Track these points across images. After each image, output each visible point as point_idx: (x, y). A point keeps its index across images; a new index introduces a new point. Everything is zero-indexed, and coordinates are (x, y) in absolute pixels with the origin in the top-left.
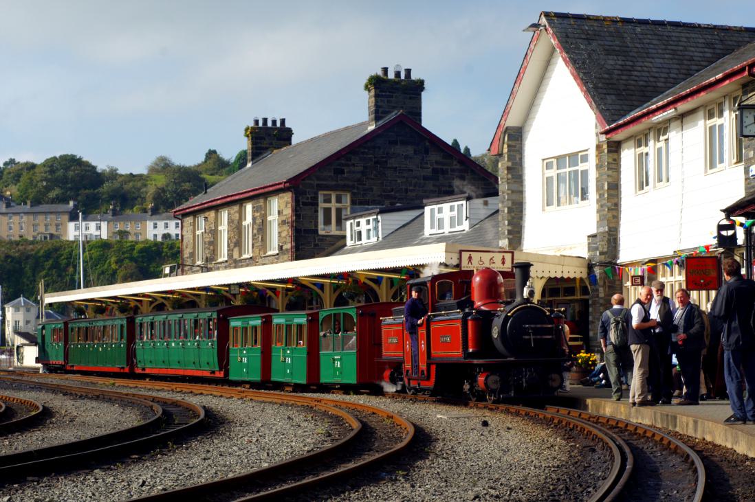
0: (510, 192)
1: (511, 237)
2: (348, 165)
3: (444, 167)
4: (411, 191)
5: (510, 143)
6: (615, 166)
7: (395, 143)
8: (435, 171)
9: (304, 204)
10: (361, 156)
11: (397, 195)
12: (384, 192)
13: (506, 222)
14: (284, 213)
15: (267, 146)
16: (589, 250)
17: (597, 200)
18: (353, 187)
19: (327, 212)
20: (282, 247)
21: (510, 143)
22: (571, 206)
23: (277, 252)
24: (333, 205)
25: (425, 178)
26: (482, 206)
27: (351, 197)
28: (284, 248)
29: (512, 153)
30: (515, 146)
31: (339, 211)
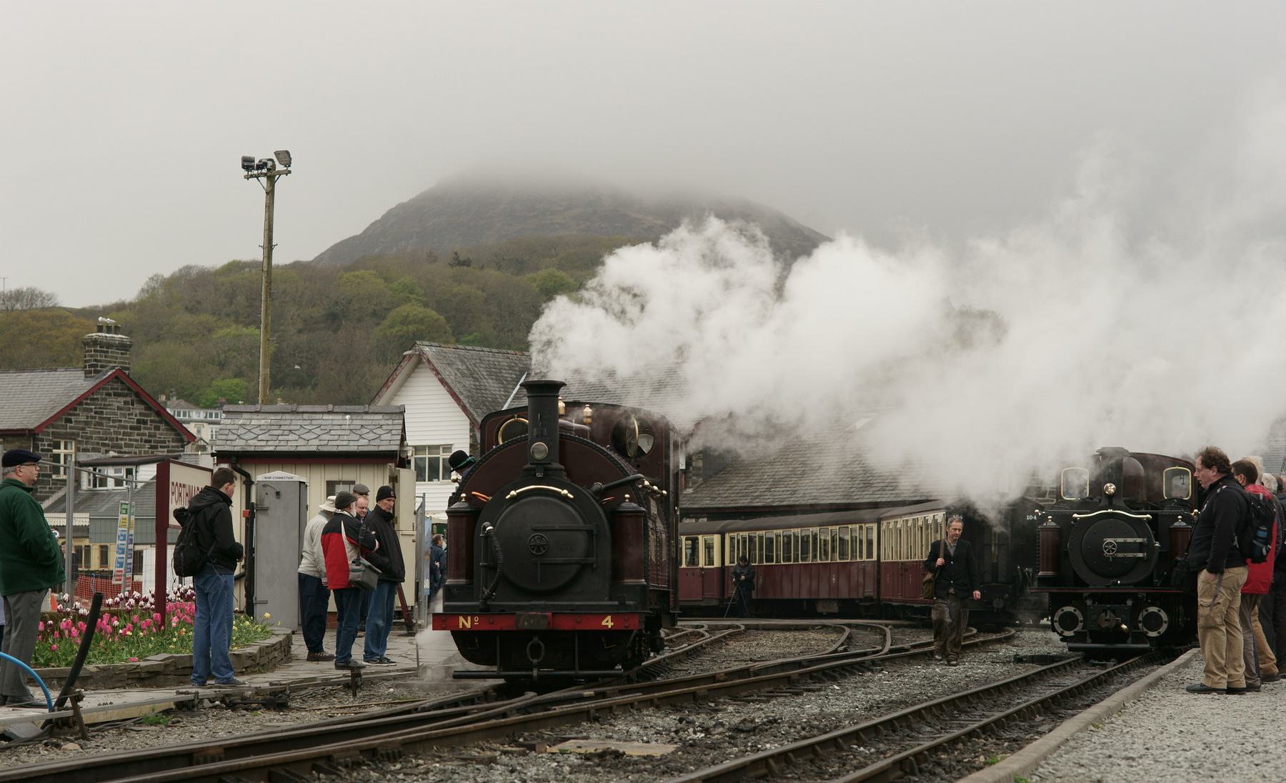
2: (74, 415)
3: (146, 418)
4: (121, 439)
7: (109, 395)
8: (138, 421)
9: (42, 450)
10: (84, 406)
24: (62, 451)
25: (131, 428)
27: (76, 445)
31: (65, 456)
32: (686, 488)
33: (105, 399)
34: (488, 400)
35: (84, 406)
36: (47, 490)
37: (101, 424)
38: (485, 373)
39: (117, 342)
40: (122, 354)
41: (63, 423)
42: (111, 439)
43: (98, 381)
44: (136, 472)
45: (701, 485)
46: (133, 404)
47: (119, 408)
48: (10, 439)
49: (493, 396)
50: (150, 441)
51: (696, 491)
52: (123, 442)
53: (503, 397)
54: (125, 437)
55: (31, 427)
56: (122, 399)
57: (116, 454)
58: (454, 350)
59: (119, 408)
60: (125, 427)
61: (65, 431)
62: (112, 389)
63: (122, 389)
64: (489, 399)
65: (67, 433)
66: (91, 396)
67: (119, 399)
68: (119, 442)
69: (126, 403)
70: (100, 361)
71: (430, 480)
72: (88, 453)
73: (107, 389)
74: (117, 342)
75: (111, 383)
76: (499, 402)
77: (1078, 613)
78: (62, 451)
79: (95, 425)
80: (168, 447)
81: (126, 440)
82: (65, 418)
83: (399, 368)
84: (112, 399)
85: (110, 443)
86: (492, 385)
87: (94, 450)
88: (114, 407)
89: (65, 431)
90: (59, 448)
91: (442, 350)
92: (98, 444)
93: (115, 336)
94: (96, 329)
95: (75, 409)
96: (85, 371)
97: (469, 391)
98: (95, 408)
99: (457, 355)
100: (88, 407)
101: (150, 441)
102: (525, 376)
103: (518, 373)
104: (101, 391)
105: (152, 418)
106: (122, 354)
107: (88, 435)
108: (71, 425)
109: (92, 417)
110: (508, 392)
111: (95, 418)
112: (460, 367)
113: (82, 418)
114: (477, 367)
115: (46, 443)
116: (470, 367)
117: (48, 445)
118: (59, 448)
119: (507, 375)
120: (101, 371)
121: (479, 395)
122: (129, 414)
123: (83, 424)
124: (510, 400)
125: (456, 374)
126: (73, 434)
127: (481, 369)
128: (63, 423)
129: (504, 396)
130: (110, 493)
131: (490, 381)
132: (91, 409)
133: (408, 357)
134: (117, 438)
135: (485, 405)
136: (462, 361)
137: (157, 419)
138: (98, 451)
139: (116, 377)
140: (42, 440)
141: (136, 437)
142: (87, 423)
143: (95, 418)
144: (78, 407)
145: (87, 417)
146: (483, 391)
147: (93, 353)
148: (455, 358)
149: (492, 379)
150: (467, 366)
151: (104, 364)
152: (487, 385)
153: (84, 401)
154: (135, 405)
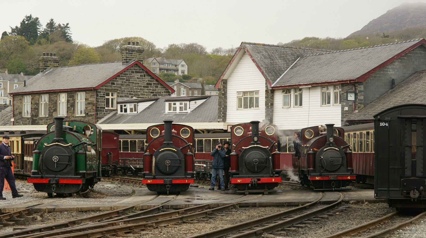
0: (223, 102)
1: (223, 118)
2: (116, 81)
3: (151, 83)
4: (139, 92)
5: (223, 85)
6: (272, 98)
7: (133, 72)
9: (100, 97)
10: (121, 77)
11: (134, 93)
12: (129, 92)
13: (222, 113)
14: (89, 100)
15: (49, 65)
18: (118, 90)
19: (108, 99)
20: (87, 114)
21: (223, 85)
23: (84, 115)
24: (110, 97)
25: (144, 87)
26: (194, 104)
27: (117, 94)
28: (89, 114)
29: (224, 88)
31: (112, 99)
32: (355, 110)
33: (131, 74)
34: (276, 70)
35: (121, 77)
36: (103, 114)
37: (129, 85)
38: (277, 57)
39: (137, 49)
40: (139, 54)
41: (111, 85)
42: (134, 92)
43: (127, 66)
44: (138, 106)
45: (362, 108)
46: (144, 76)
47: (138, 78)
48: (88, 92)
49: (280, 68)
50: (153, 93)
51: (359, 112)
52: (140, 93)
53: (285, 68)
54: (141, 91)
55: (94, 86)
56: (139, 74)
57: (137, 98)
58: (263, 46)
59: (138, 78)
60: (140, 86)
61: (111, 88)
62: (134, 69)
63: (139, 70)
64: (277, 69)
65: (112, 89)
66: (124, 73)
67: (138, 74)
68: (138, 93)
69: (141, 76)
70: (128, 57)
71: (250, 107)
72: (123, 98)
73: (132, 70)
74: (137, 49)
75: (134, 67)
78: (110, 97)
79: (126, 85)
80: (162, 95)
81: (141, 92)
82: (111, 83)
84: (135, 74)
85: (134, 93)
87: (125, 96)
88: (135, 78)
89: (111, 88)
90: (109, 96)
92: (128, 94)
93: (136, 46)
94: (127, 43)
95: (116, 79)
96: (122, 62)
98: (126, 78)
99: (264, 49)
100: (122, 77)
101: (153, 93)
104: (129, 71)
105: (154, 82)
106: (139, 54)
107: (123, 90)
108: (114, 85)
109: (125, 82)
111: (126, 82)
112: (265, 54)
113: (120, 82)
114: (273, 54)
115: (102, 94)
117: (103, 94)
118: (109, 96)
119: (290, 58)
120: (129, 62)
121: (272, 67)
122: (143, 81)
123: (121, 85)
124: (289, 69)
126: (115, 89)
128: (111, 85)
130: (128, 115)
131: (280, 60)
132: (124, 79)
134: (137, 91)
136: (266, 51)
137: (157, 83)
138: (128, 97)
139: (136, 64)
140: (100, 92)
141: (147, 91)
142: (122, 85)
143: (126, 82)
144: (118, 77)
145: (122, 82)
147: (125, 54)
149: (281, 60)
150: (268, 54)
151: (130, 59)
152: (278, 62)
153: (121, 75)
154: (146, 77)
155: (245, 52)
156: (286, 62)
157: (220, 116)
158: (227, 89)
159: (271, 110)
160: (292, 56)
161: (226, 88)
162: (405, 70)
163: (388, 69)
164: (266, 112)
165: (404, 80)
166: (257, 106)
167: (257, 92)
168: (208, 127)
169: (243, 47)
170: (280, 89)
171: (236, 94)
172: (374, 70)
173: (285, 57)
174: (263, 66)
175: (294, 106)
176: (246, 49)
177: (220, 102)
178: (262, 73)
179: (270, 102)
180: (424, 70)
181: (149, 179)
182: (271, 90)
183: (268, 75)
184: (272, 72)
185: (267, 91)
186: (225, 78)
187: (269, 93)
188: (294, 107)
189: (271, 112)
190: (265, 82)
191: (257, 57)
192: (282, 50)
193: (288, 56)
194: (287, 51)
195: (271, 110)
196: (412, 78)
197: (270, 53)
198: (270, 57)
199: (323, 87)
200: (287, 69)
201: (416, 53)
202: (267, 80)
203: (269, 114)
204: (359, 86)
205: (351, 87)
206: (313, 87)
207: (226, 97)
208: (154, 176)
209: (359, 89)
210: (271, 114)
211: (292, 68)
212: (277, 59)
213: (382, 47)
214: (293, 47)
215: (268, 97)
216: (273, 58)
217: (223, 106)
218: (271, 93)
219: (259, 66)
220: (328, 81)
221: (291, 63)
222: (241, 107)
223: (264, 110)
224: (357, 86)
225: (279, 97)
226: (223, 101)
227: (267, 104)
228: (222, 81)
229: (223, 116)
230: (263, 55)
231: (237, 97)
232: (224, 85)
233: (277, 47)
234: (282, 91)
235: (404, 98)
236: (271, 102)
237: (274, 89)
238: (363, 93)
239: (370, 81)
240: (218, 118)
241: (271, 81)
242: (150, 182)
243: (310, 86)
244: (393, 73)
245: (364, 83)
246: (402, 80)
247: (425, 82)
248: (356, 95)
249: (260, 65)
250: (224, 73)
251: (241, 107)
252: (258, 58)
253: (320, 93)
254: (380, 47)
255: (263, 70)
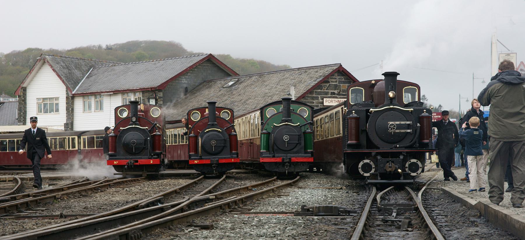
1: (23, 122)
6: (73, 103)
13: (22, 117)
16: (65, 128)
17: (66, 113)
22: (50, 113)
30: (24, 93)
34: (74, 79)
38: (74, 67)
49: (77, 77)
53: (81, 77)
58: (60, 57)
64: (75, 78)
76: (79, 79)
77: (372, 163)
83: (35, 65)
86: (77, 72)
91: (54, 58)
97: (66, 74)
99: (61, 60)
102: (92, 69)
103: (89, 68)
110: (84, 75)
112: (63, 65)
114: (70, 64)
116: (67, 65)
121: (70, 76)
124: (85, 78)
125: (60, 67)
127: (72, 66)
129: (82, 77)
131: (76, 70)
133: (39, 60)
135: (73, 81)
136: (63, 62)
146: (72, 75)
148: (60, 61)
149: (77, 70)
150: (66, 64)
152: (74, 72)
155: (44, 62)
156: (82, 72)
157: (21, 121)
158: (26, 96)
159: (71, 115)
160: (86, 67)
161: (26, 95)
162: (195, 80)
163: (182, 78)
164: (66, 116)
165: (195, 88)
166: (57, 110)
167: (57, 99)
168: (15, 130)
169: (43, 58)
170: (81, 96)
171: (36, 101)
172: (172, 79)
173: (80, 68)
174: (63, 75)
175: (95, 110)
176: (46, 60)
177: (20, 108)
178: (63, 82)
179: (70, 107)
180: (212, 80)
181: (196, 159)
182: (71, 97)
183: (68, 83)
184: (71, 81)
185: (67, 98)
186: (24, 85)
187: (69, 99)
188: (95, 112)
189: (72, 116)
190: (65, 90)
191: (57, 67)
192: (77, 62)
193: (83, 67)
194: (81, 62)
195: (71, 115)
196: (202, 86)
197: (67, 64)
198: (68, 68)
199: (123, 94)
200: (83, 79)
201: (204, 66)
202: (67, 88)
203: (70, 118)
204: (159, 93)
205: (151, 94)
206: (114, 94)
207: (25, 103)
208: (201, 156)
209: (159, 95)
210: (71, 118)
211: (88, 77)
212: (74, 70)
213: (172, 60)
214: (85, 59)
215: (68, 103)
216: (70, 68)
217: (23, 111)
218: (72, 99)
219: (59, 75)
220: (130, 89)
221: (85, 73)
222: (41, 112)
223: (65, 115)
224: (157, 93)
225: (79, 103)
226: (23, 107)
227: (67, 109)
228: (21, 89)
229: (23, 120)
230: (61, 65)
231: (37, 103)
232: (24, 92)
233: (72, 59)
234: (82, 97)
235: (200, 103)
236: (72, 107)
237: (74, 95)
238: (162, 99)
239: (167, 89)
240: (18, 122)
241: (72, 89)
242: (197, 162)
243: (112, 93)
244: (186, 82)
245: (163, 90)
246: (193, 88)
247: (215, 89)
248: (156, 100)
249: (60, 74)
250: (24, 81)
251: (41, 112)
252: (58, 68)
253: (121, 99)
254: (171, 60)
255: (63, 79)
